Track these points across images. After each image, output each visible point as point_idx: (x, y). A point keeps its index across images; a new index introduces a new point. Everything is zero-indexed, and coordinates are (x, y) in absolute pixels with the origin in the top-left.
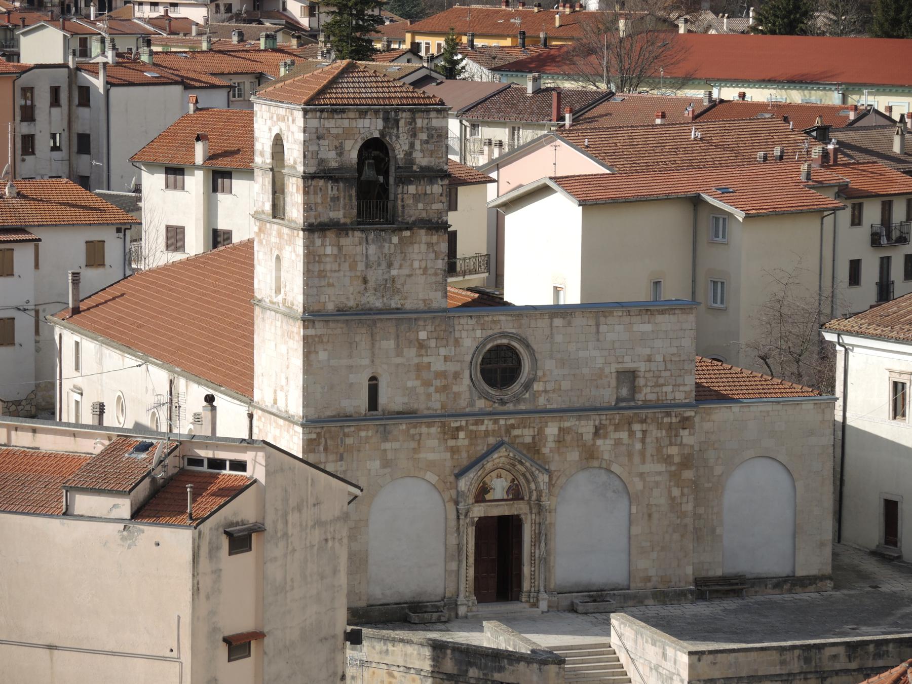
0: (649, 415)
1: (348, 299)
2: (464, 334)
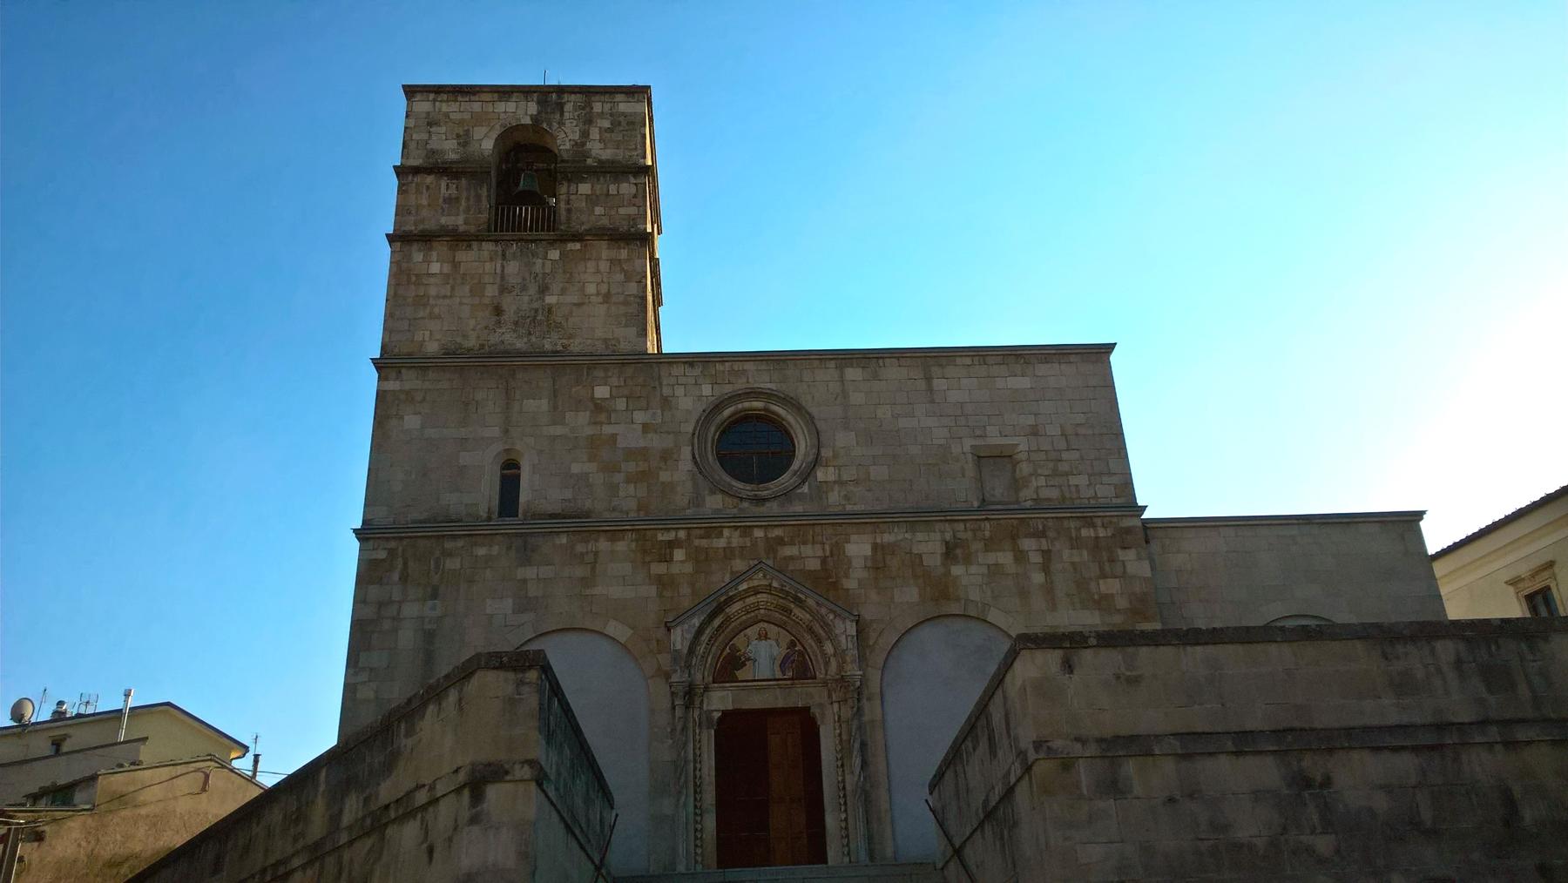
0: (1050, 523)
1: (465, 336)
2: (680, 391)
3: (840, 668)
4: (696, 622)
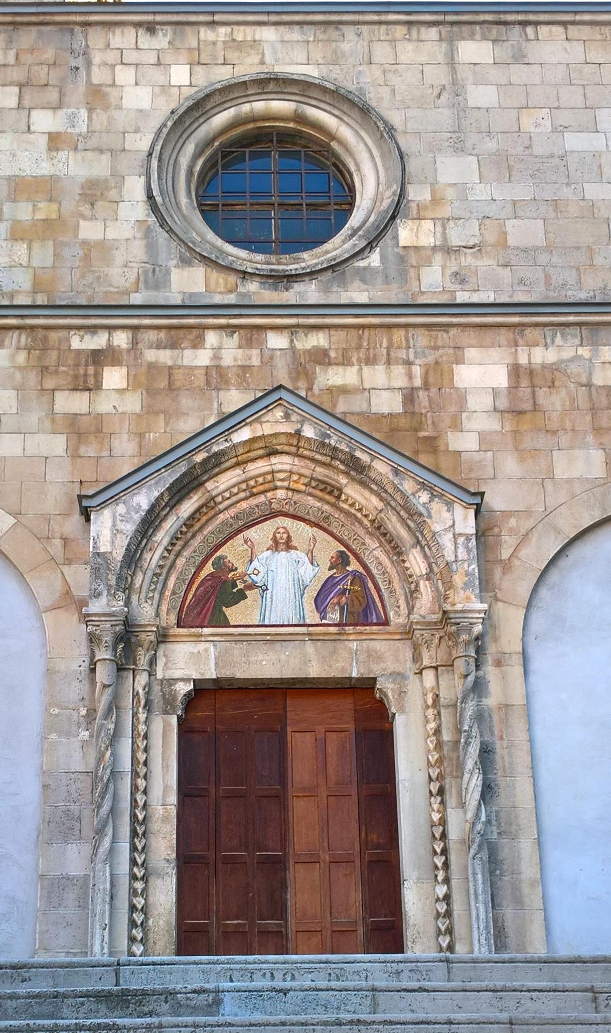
2: (125, 76)
3: (441, 597)
4: (143, 500)
